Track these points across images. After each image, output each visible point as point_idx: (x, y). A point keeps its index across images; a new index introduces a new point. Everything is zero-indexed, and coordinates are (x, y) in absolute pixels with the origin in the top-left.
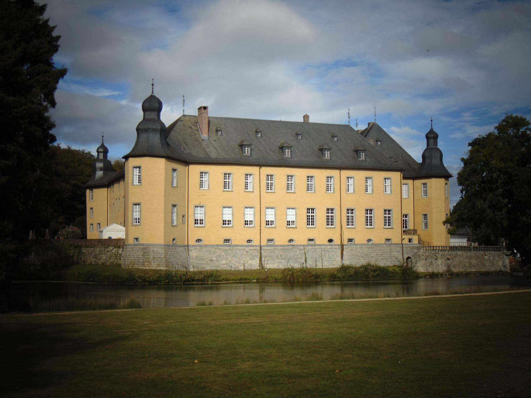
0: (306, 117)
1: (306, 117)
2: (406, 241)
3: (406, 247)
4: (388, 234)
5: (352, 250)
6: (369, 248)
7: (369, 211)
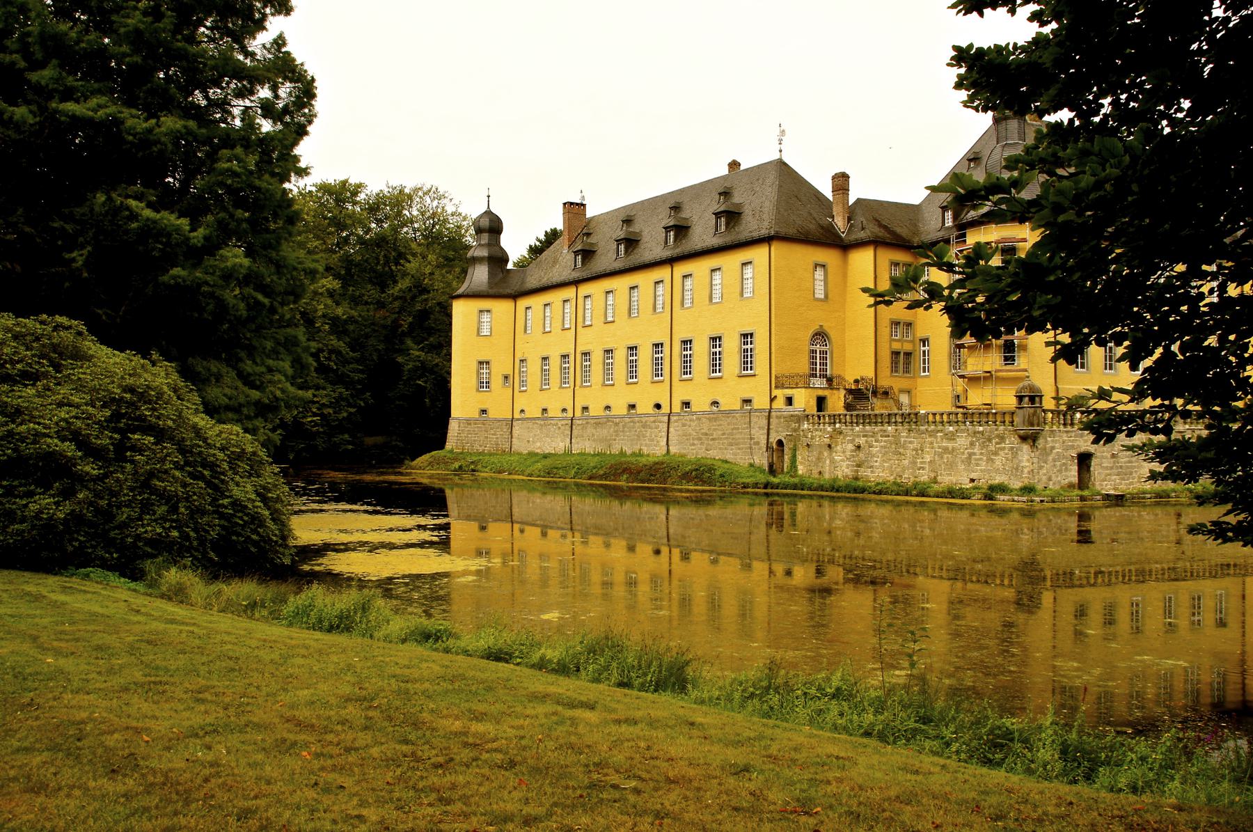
0: (734, 165)
1: (734, 165)
2: (780, 403)
3: (777, 417)
4: (748, 388)
5: (684, 425)
6: (710, 419)
7: (715, 340)
